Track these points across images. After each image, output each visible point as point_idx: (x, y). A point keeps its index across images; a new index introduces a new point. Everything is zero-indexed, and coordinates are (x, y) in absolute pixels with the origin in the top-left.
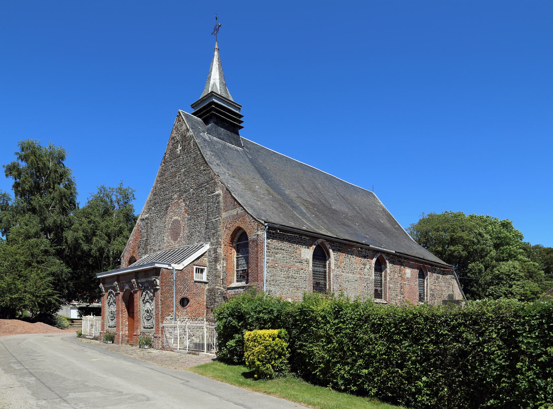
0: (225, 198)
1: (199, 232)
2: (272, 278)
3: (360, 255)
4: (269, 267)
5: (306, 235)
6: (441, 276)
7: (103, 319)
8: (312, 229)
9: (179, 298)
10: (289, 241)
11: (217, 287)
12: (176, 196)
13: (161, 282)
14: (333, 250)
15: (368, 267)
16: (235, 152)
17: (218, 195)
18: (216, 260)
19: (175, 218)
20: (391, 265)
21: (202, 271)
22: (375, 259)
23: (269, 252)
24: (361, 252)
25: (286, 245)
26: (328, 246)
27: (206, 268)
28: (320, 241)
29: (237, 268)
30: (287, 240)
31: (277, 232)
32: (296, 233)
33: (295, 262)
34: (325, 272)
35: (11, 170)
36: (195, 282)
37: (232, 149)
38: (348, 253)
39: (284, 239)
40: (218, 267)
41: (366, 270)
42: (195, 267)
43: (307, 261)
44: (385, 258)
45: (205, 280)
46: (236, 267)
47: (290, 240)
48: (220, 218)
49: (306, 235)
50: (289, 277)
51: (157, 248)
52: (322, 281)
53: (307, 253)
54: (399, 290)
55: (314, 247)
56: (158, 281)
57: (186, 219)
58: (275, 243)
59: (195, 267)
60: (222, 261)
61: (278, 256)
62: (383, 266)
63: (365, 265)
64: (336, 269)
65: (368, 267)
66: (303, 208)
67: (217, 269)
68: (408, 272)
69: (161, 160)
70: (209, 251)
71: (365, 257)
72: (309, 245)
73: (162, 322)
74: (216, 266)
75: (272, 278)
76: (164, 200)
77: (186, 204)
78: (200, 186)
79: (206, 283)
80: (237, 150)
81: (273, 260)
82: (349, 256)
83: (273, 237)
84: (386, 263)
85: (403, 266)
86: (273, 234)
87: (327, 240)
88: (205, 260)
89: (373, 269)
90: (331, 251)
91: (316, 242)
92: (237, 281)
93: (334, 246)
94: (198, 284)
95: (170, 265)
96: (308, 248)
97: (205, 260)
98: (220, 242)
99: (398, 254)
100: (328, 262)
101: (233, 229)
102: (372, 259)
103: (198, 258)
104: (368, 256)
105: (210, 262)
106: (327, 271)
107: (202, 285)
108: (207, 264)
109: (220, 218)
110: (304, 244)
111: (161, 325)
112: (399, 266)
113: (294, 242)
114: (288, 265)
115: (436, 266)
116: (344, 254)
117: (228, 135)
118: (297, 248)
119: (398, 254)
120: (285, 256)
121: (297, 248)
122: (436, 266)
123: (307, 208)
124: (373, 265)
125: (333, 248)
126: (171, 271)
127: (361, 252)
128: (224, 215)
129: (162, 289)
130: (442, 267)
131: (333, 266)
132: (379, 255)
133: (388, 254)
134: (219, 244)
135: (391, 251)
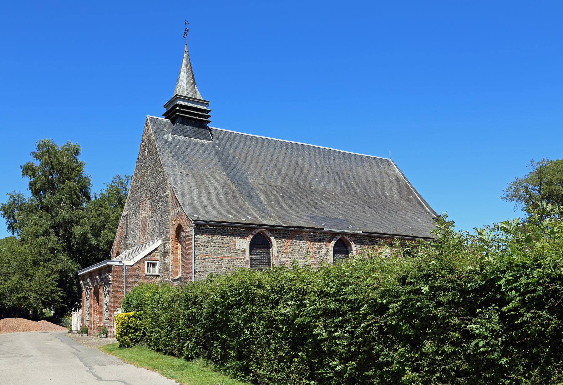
0: (172, 197)
2: (202, 269)
3: (311, 239)
4: (198, 259)
5: (241, 227)
8: (257, 219)
10: (221, 234)
11: (165, 279)
12: (144, 195)
13: (113, 278)
14: (276, 238)
15: (324, 250)
16: (200, 147)
17: (167, 196)
18: (165, 254)
19: (144, 215)
20: (358, 246)
21: (154, 265)
22: (333, 243)
23: (199, 246)
24: (315, 236)
25: (217, 238)
26: (269, 235)
27: (158, 262)
28: (258, 231)
30: (218, 233)
31: (202, 227)
33: (229, 253)
34: (269, 259)
35: (28, 170)
36: (146, 275)
37: (195, 144)
38: (296, 239)
39: (215, 233)
40: (167, 261)
41: (321, 254)
42: (146, 262)
43: (243, 251)
44: (349, 239)
45: (157, 273)
48: (168, 216)
49: (241, 227)
50: (221, 267)
51: (133, 244)
53: (243, 244)
55: (251, 237)
56: (110, 277)
58: (205, 237)
59: (146, 262)
60: (170, 255)
62: (349, 248)
63: (320, 249)
64: (280, 256)
65: (324, 250)
66: (262, 197)
67: (165, 263)
68: (386, 251)
69: (136, 161)
71: (320, 241)
72: (244, 236)
73: (113, 313)
75: (202, 269)
76: (138, 198)
78: (158, 185)
79: (158, 276)
80: (203, 145)
81: (203, 253)
82: (298, 241)
83: (203, 232)
84: (350, 244)
87: (267, 229)
88: (158, 255)
89: (332, 252)
90: (272, 239)
91: (253, 232)
93: (277, 234)
94: (150, 278)
95: (121, 262)
96: (244, 238)
97: (158, 255)
98: (169, 238)
99: (366, 234)
100: (271, 249)
101: (176, 226)
102: (330, 242)
103: (150, 254)
105: (161, 257)
107: (154, 278)
108: (159, 258)
109: (168, 216)
110: (239, 235)
113: (227, 235)
114: (220, 256)
116: (291, 241)
117: (194, 131)
118: (230, 240)
119: (366, 234)
120: (217, 248)
121: (230, 240)
123: (268, 195)
124: (332, 249)
125: (276, 236)
127: (315, 236)
128: (172, 213)
129: (113, 284)
131: (276, 254)
133: (353, 236)
134: (167, 240)
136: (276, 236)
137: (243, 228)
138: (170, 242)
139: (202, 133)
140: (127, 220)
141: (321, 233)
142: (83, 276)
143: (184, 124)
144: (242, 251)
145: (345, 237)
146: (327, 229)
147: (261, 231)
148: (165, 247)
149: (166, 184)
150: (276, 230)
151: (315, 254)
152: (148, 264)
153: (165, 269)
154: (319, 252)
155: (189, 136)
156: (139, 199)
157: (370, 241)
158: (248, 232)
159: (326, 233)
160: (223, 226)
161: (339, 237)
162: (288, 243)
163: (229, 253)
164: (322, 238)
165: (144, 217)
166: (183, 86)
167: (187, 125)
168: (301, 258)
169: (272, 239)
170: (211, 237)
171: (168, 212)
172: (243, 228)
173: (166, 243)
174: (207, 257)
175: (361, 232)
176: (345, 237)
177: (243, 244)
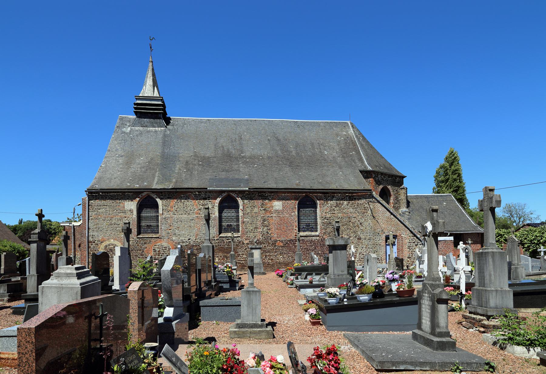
2: (95, 226)
3: (197, 198)
5: (129, 192)
6: (346, 202)
10: (112, 199)
14: (161, 199)
22: (219, 200)
25: (109, 202)
26: (155, 197)
32: (118, 192)
33: (119, 213)
37: (149, 132)
38: (181, 198)
43: (131, 211)
47: (113, 198)
49: (129, 192)
50: (111, 224)
52: (235, 224)
53: (131, 205)
54: (259, 224)
55: (138, 199)
58: (98, 202)
61: (101, 210)
64: (165, 213)
68: (277, 205)
71: (205, 199)
72: (132, 199)
75: (95, 226)
80: (156, 131)
81: (96, 214)
85: (268, 199)
86: (96, 196)
90: (158, 200)
91: (140, 196)
96: (132, 201)
102: (216, 199)
104: (209, 197)
110: (128, 199)
112: (260, 202)
113: (117, 199)
115: (336, 193)
116: (176, 200)
119: (252, 190)
122: (334, 193)
124: (217, 205)
125: (162, 197)
130: (347, 193)
132: (224, 195)
135: (244, 189)
136: (162, 197)
137: (131, 192)
139: (157, 123)
141: (206, 192)
143: (142, 118)
144: (130, 211)
145: (232, 194)
146: (211, 188)
147: (147, 194)
150: (161, 192)
155: (146, 126)
157: (260, 196)
158: (135, 196)
159: (211, 192)
160: (113, 192)
161: (224, 195)
162: (173, 202)
163: (119, 213)
164: (207, 196)
166: (148, 90)
167: (144, 118)
168: (185, 214)
169: (158, 200)
170: (103, 202)
172: (131, 192)
175: (247, 189)
176: (232, 194)
177: (131, 205)
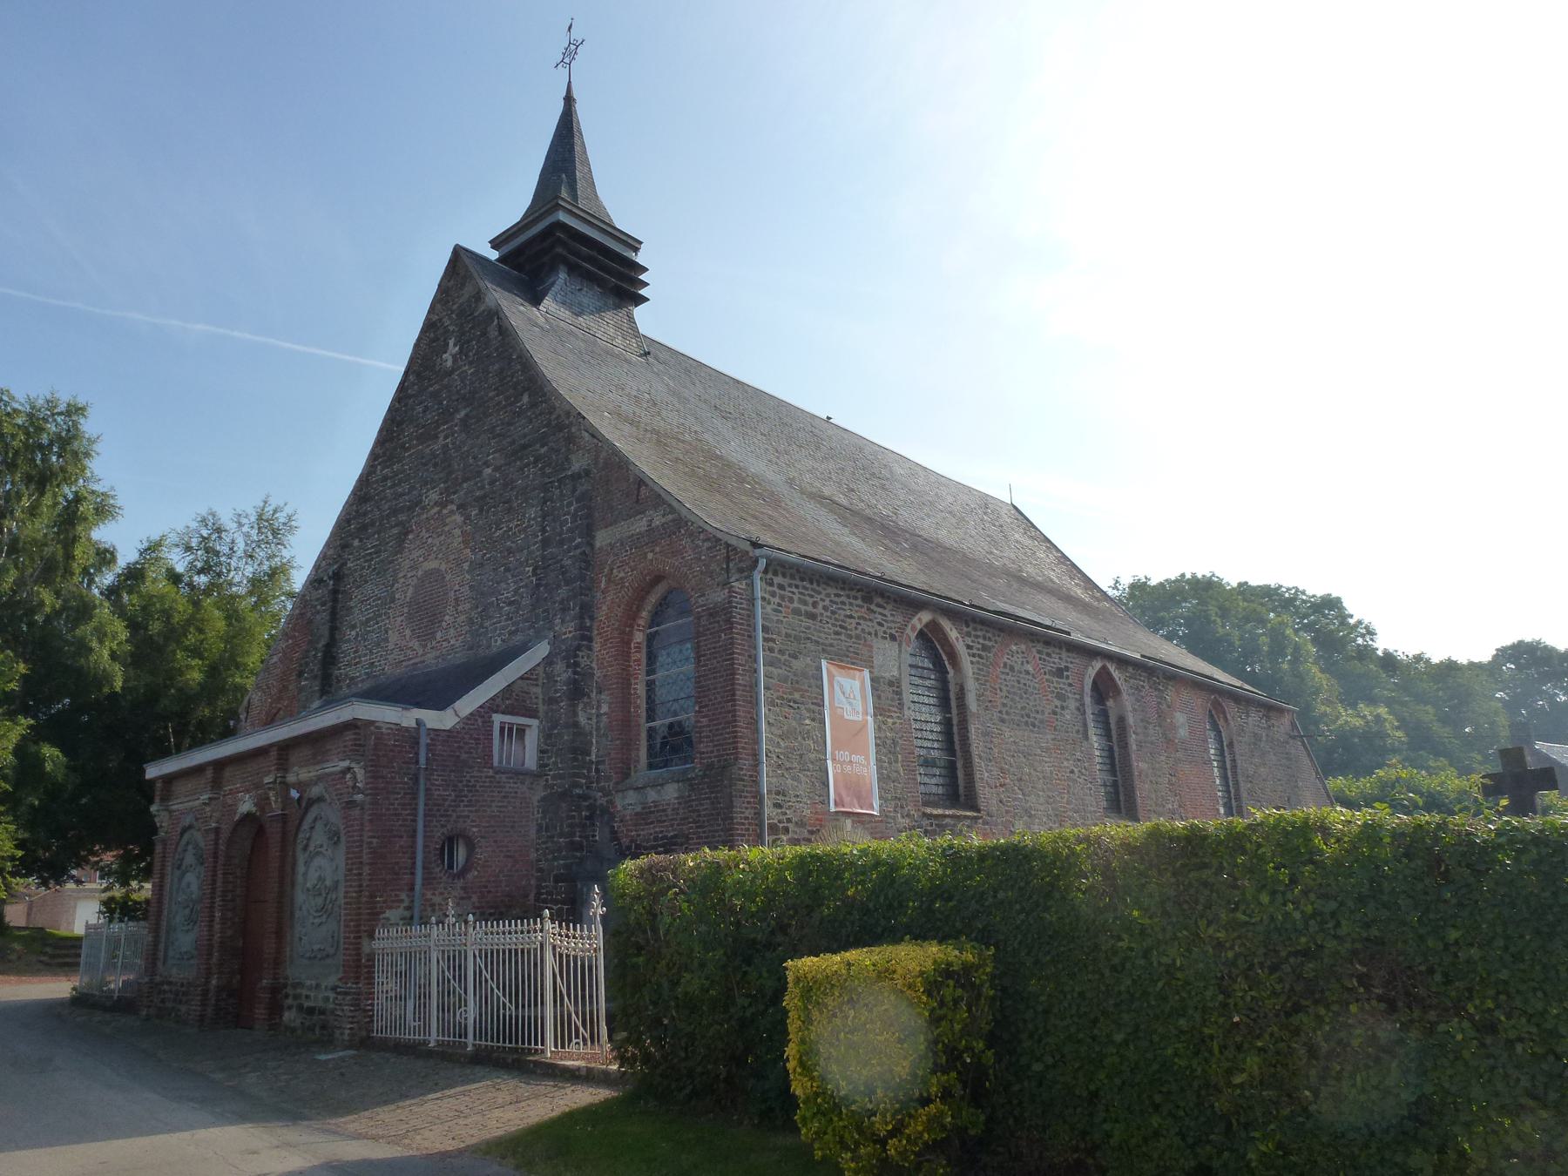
1: (510, 603)
7: (156, 930)
9: (438, 834)
18: (577, 691)
21: (521, 731)
27: (535, 722)
29: (650, 718)
40: (582, 719)
46: (643, 712)
57: (466, 566)
59: (498, 719)
60: (593, 695)
67: (576, 724)
70: (548, 661)
71: (1060, 673)
73: (371, 937)
74: (575, 714)
77: (468, 517)
84: (1118, 692)
90: (960, 647)
91: (915, 621)
92: (651, 766)
93: (968, 634)
96: (893, 638)
98: (590, 629)
105: (551, 701)
106: (955, 722)
108: (542, 708)
111: (366, 949)
125: (969, 641)
126: (411, 737)
128: (602, 538)
134: (583, 638)
138: (596, 646)
140: (335, 592)
142: (169, 779)
144: (891, 684)
148: (576, 664)
149: (570, 439)
151: (1055, 713)
152: (502, 729)
153: (574, 750)
154: (1063, 708)
156: (402, 517)
165: (429, 573)
171: (589, 532)
173: (579, 648)
174: (797, 696)
